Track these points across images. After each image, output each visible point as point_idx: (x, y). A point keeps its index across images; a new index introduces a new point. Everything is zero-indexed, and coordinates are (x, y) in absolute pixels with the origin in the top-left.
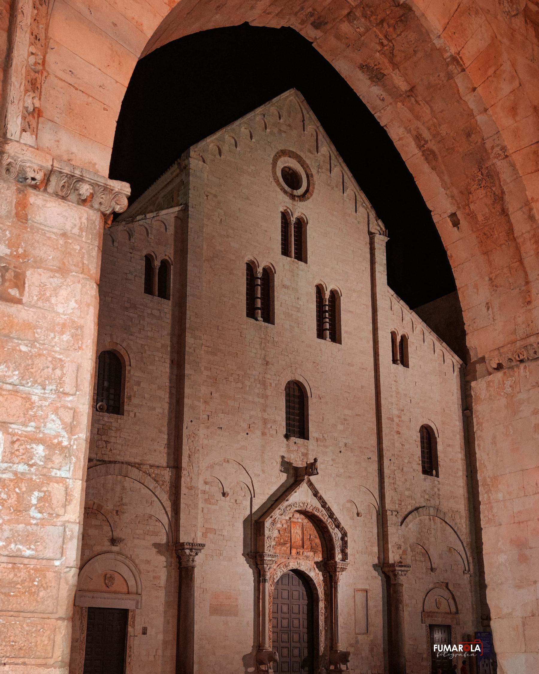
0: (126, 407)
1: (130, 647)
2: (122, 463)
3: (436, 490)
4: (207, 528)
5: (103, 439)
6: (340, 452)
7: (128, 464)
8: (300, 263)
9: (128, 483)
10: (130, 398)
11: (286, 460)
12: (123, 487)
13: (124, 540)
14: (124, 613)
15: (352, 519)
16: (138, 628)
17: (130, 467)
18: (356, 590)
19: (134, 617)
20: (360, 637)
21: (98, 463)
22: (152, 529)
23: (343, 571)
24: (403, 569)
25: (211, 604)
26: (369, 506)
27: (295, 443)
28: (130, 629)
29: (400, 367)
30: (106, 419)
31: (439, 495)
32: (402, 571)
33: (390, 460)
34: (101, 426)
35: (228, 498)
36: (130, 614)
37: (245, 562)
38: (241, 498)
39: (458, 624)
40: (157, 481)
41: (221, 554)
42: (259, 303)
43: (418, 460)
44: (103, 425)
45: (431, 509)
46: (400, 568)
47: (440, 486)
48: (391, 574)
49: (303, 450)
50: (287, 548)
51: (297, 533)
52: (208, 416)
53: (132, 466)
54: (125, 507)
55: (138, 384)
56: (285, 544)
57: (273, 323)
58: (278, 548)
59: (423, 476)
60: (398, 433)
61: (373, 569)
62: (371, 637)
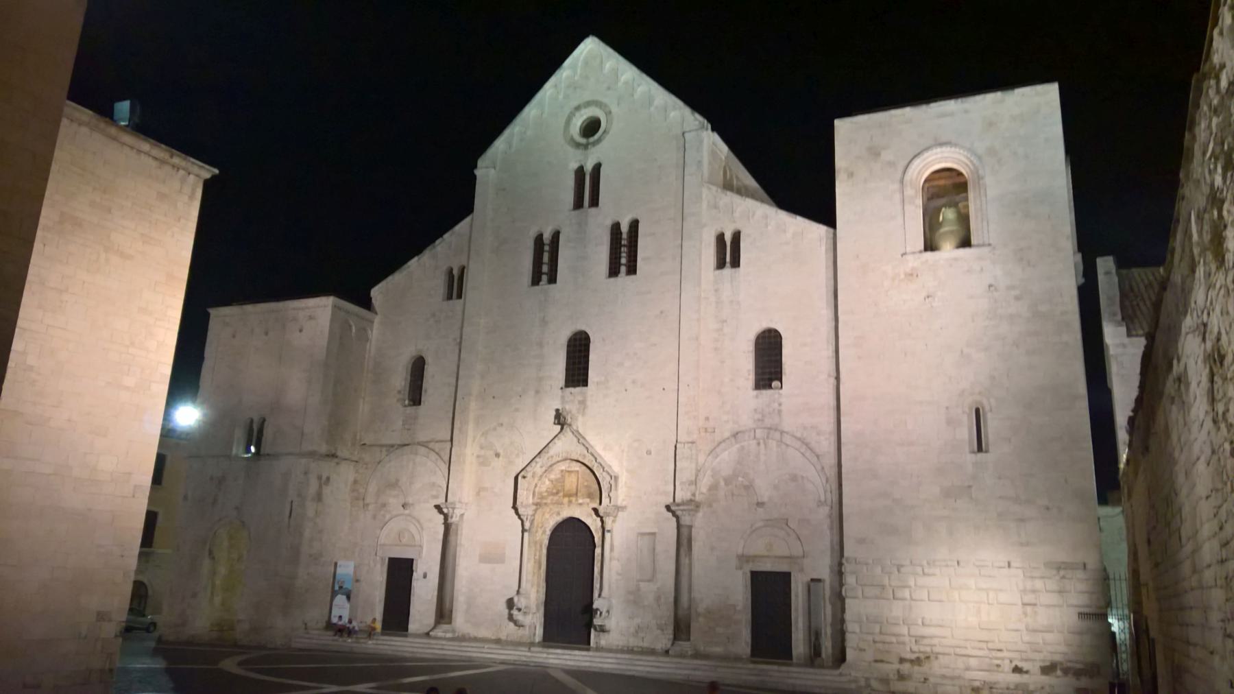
3: (776, 405)
10: (426, 391)
14: (411, 561)
18: (643, 534)
19: (417, 565)
20: (642, 585)
24: (681, 508)
35: (501, 458)
36: (415, 562)
39: (802, 570)
42: (545, 268)
47: (783, 400)
49: (580, 398)
51: (572, 481)
55: (433, 376)
56: (557, 493)
59: (756, 392)
61: (665, 510)
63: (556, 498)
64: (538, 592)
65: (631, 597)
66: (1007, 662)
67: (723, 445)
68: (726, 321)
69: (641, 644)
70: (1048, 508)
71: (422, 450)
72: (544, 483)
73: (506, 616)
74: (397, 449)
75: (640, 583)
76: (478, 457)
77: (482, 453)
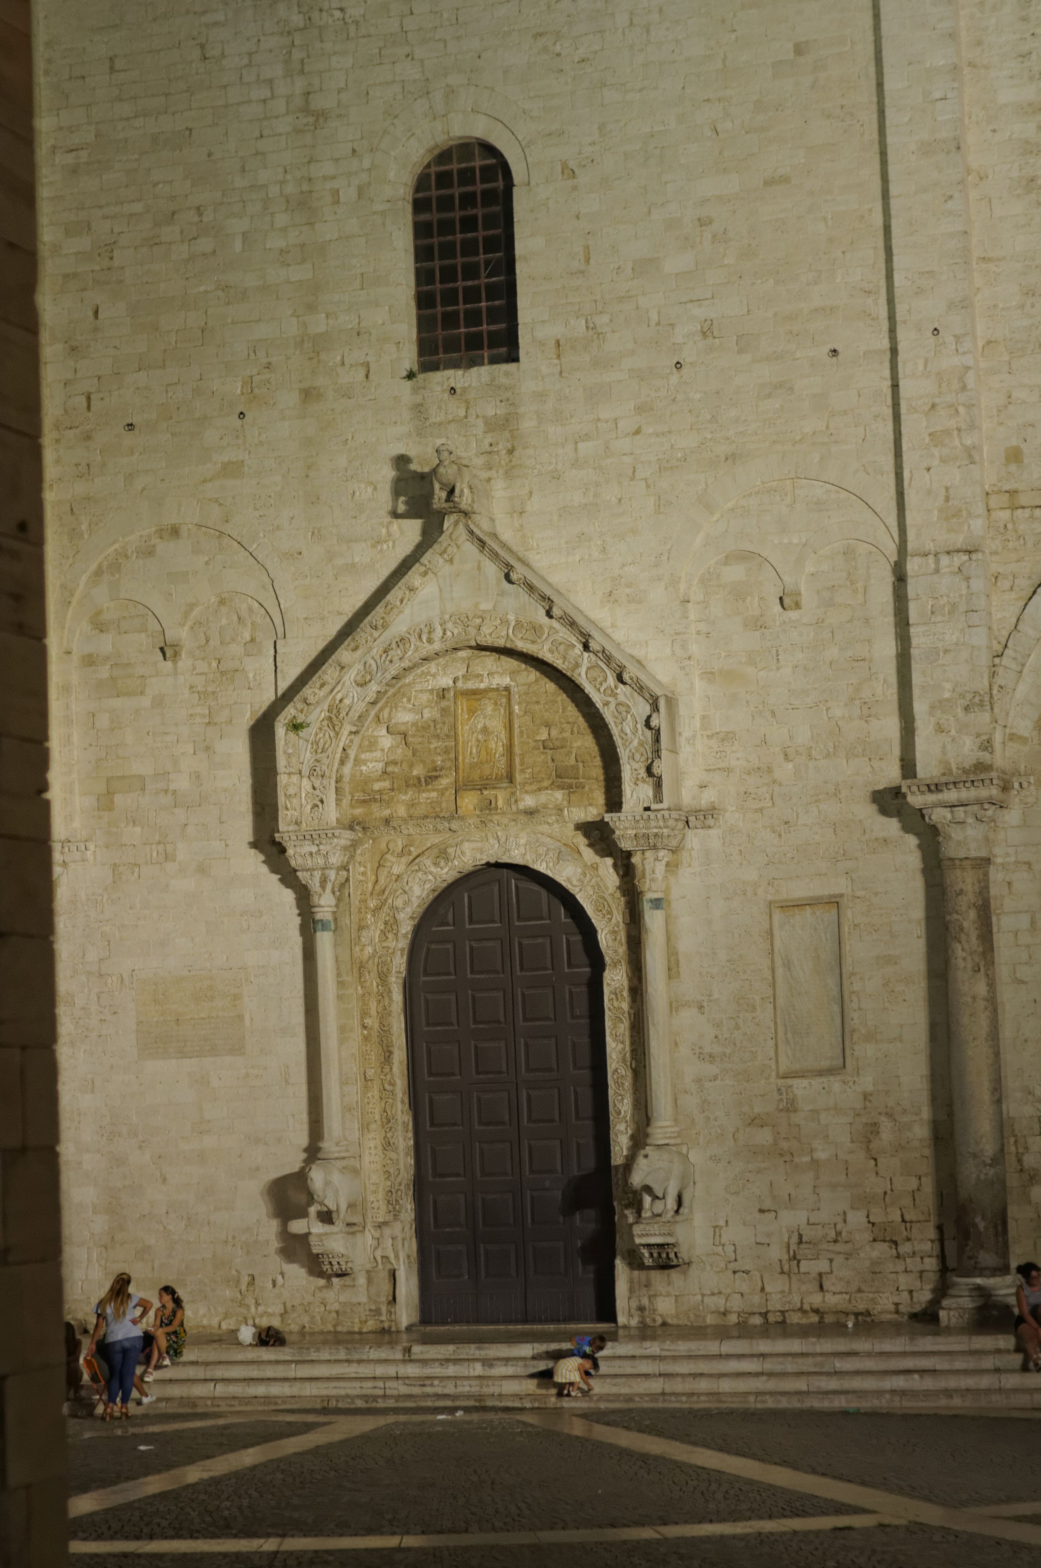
4: (108, 780)
6: (678, 365)
11: (413, 467)
15: (758, 624)
24: (951, 795)
25: (139, 1023)
26: (848, 553)
35: (184, 662)
37: (265, 869)
38: (236, 649)
41: (168, 857)
46: (931, 798)
50: (442, 793)
51: (485, 730)
56: (431, 778)
61: (874, 808)
62: (867, 1082)
63: (428, 796)
64: (388, 1145)
65: (764, 1137)
69: (816, 1299)
72: (372, 745)
73: (276, 1244)
75: (800, 1087)
76: (89, 661)
77: (106, 644)
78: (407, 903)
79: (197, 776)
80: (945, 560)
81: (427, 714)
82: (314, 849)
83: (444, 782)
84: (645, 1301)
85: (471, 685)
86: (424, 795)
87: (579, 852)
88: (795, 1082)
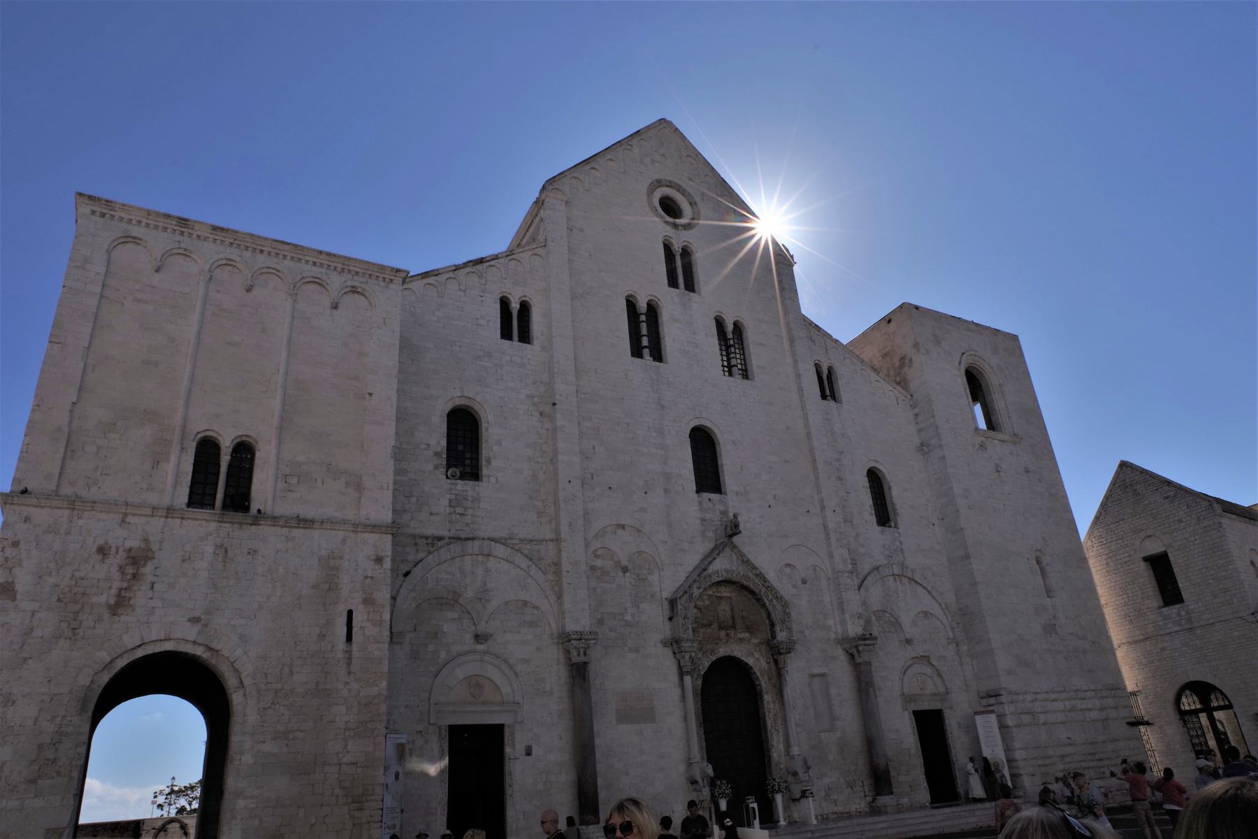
0: (485, 471)
1: (510, 774)
2: (483, 539)
3: (897, 543)
5: (457, 511)
6: (770, 506)
7: (491, 539)
8: (692, 294)
9: (492, 563)
10: (489, 461)
12: (487, 568)
13: (491, 635)
14: (500, 728)
15: (795, 586)
16: (520, 748)
17: (493, 543)
21: (452, 540)
22: (528, 618)
23: (789, 652)
24: (867, 642)
25: (617, 709)
27: (710, 499)
28: (508, 750)
29: (832, 404)
30: (459, 487)
31: (902, 549)
32: (865, 645)
33: (834, 511)
34: (453, 497)
38: (645, 572)
40: (531, 559)
42: (645, 341)
43: (869, 509)
44: (456, 495)
45: (895, 567)
46: (863, 642)
47: (902, 539)
48: (854, 651)
49: (722, 508)
51: (724, 610)
52: (592, 475)
53: (496, 542)
54: (490, 593)
55: (499, 443)
56: (710, 625)
57: (667, 363)
58: (701, 630)
59: (880, 528)
60: (840, 479)
63: (709, 630)
66: (1106, 768)
67: (869, 578)
68: (843, 453)
69: (836, 809)
70: (1093, 643)
71: (500, 550)
74: (449, 544)
78: (703, 668)
79: (633, 615)
80: (847, 574)
81: (706, 602)
82: (691, 644)
83: (714, 626)
84: (790, 813)
85: (719, 595)
86: (708, 630)
87: (753, 654)
88: (823, 734)
